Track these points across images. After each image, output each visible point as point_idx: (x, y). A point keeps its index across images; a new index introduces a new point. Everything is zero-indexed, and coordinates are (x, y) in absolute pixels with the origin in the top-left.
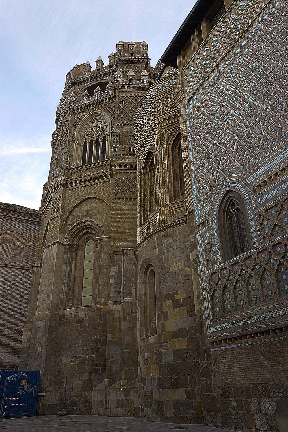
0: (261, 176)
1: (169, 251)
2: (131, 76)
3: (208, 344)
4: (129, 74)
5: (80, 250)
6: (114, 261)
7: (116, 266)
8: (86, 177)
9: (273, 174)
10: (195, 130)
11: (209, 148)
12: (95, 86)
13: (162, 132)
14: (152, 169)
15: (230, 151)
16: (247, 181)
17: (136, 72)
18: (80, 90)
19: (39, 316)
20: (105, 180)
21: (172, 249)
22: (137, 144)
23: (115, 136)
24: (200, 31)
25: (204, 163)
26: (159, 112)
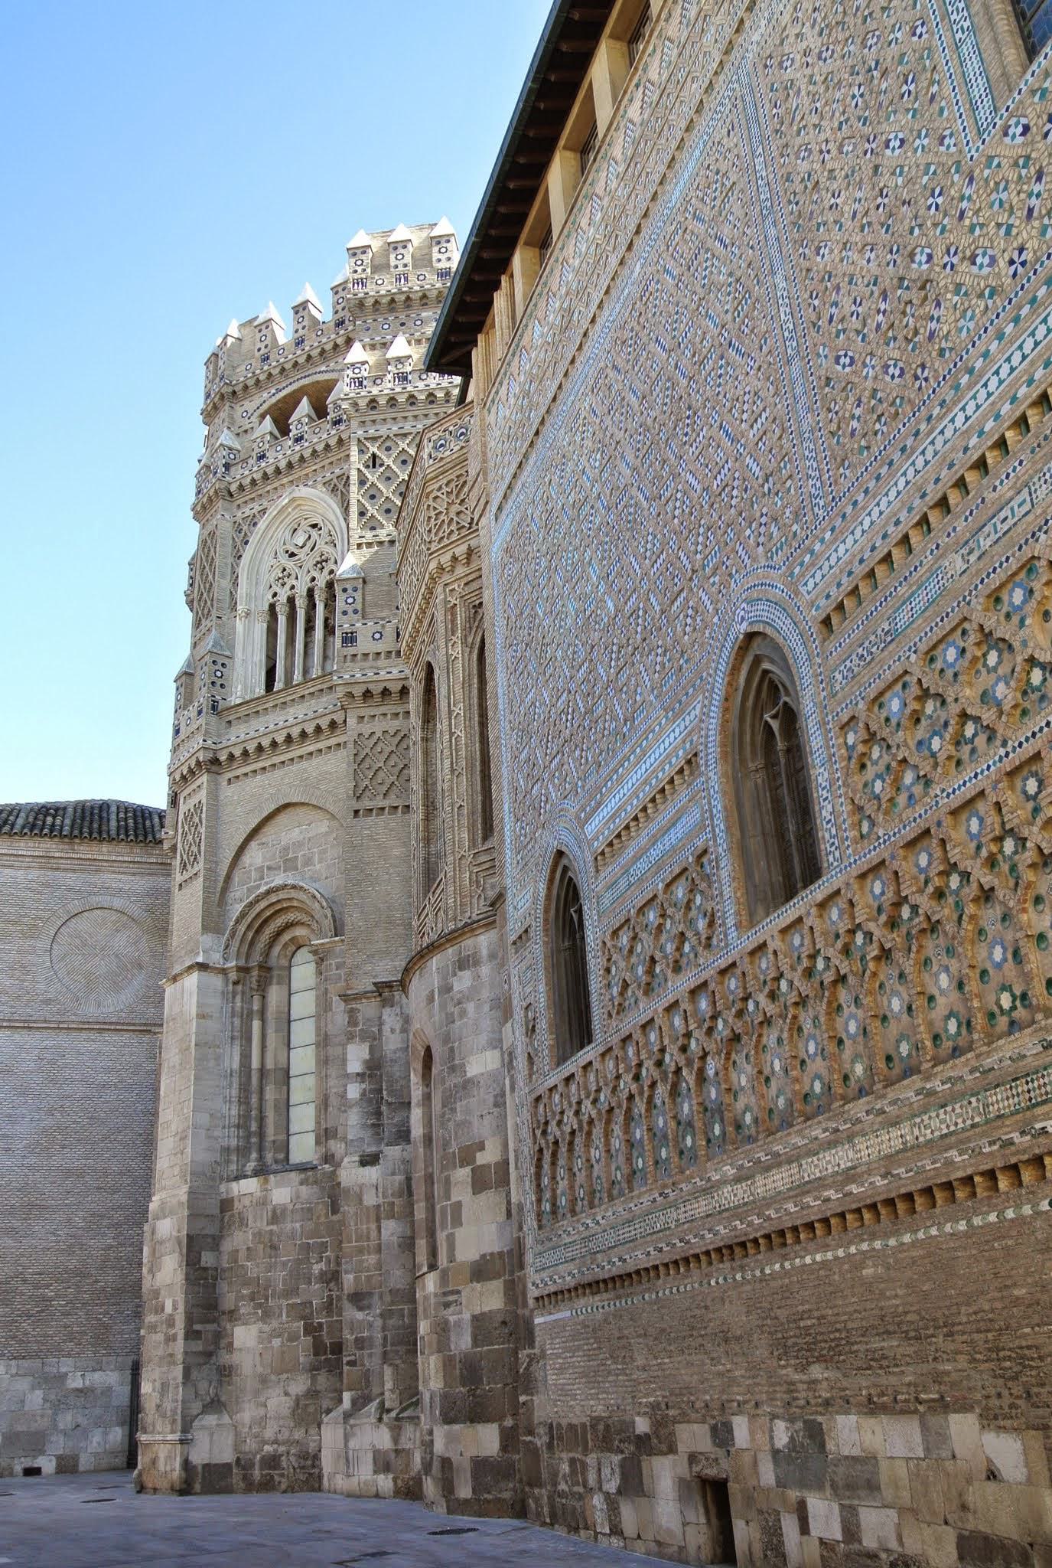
1: (463, 1013)
2: (399, 360)
3: (531, 1302)
5: (275, 980)
6: (356, 1025)
7: (363, 1039)
8: (274, 735)
19: (163, 1203)
20: (333, 741)
21: (470, 1007)
23: (350, 591)
26: (441, 534)
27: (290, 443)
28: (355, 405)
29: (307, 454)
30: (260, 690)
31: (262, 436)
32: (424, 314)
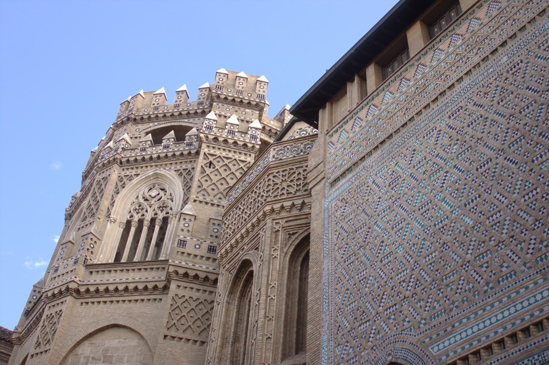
0: (458, 345)
2: (232, 124)
4: (229, 121)
9: (482, 346)
10: (338, 237)
11: (362, 274)
12: (166, 130)
13: (275, 228)
14: (246, 292)
15: (401, 287)
16: (431, 350)
17: (242, 121)
18: (140, 132)
22: (225, 242)
24: (363, 79)
25: (349, 301)
26: (275, 194)
27: (161, 148)
28: (207, 137)
29: (170, 154)
30: (112, 261)
31: (146, 141)
32: (247, 110)
